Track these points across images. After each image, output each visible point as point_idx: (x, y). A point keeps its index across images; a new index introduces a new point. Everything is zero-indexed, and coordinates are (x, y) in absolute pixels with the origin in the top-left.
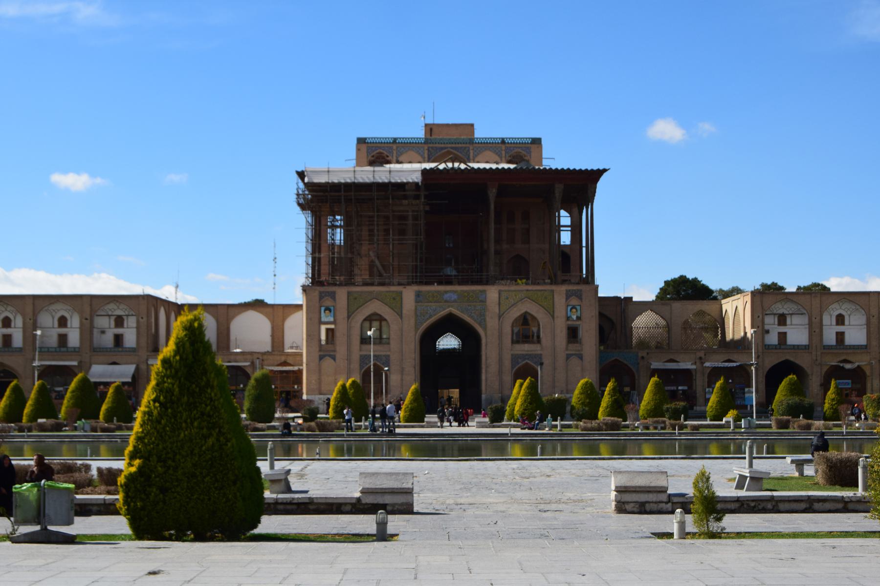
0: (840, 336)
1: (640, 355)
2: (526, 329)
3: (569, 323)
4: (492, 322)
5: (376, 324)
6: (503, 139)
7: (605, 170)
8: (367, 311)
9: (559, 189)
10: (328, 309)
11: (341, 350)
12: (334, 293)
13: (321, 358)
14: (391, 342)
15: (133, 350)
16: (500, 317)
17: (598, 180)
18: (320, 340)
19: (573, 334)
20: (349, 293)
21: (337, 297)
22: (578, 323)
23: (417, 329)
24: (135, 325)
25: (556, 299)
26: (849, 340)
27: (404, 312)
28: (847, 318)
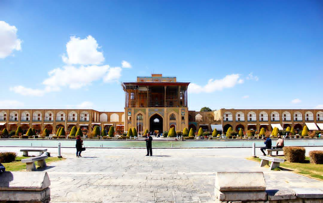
0: (239, 119)
2: (172, 118)
3: (182, 116)
4: (165, 116)
5: (140, 116)
7: (190, 83)
8: (138, 113)
9: (180, 87)
10: (130, 112)
13: (128, 123)
15: (88, 121)
16: (167, 114)
17: (188, 85)
18: (128, 119)
19: (183, 118)
22: (184, 116)
23: (149, 117)
26: (241, 120)
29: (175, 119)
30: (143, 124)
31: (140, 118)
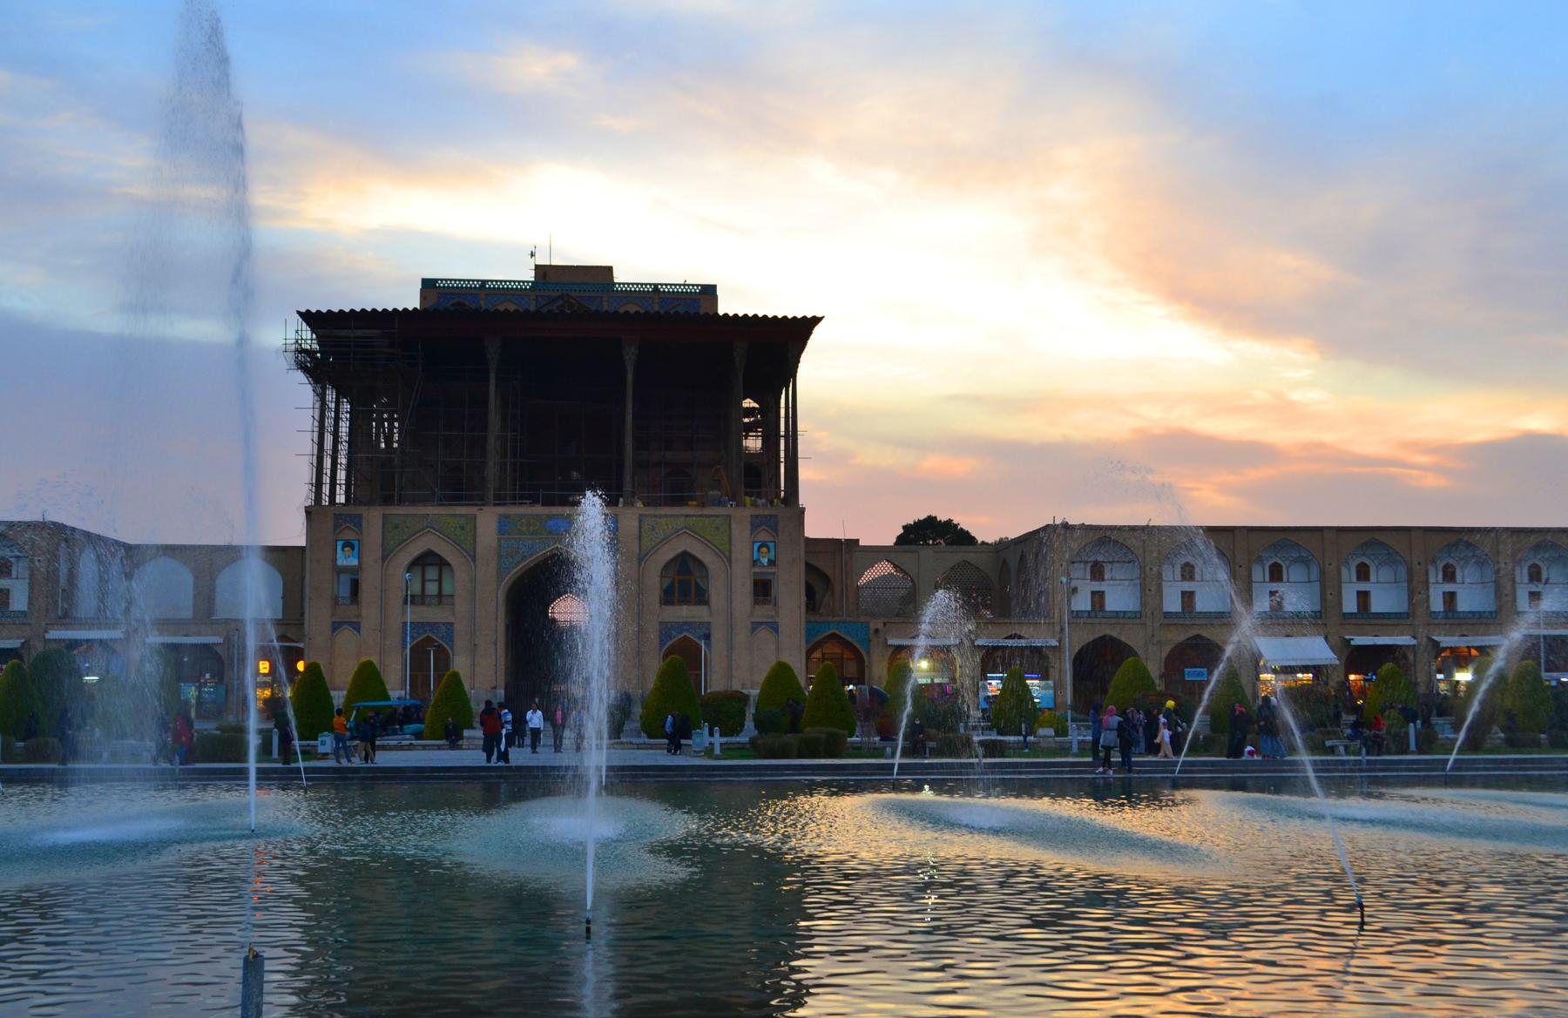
1: (872, 626)
5: (432, 573)
6: (656, 285)
8: (415, 549)
11: (369, 612)
12: (360, 516)
13: (336, 626)
14: (457, 601)
16: (640, 560)
19: (762, 590)
20: (385, 516)
21: (364, 524)
24: (27, 574)
25: (735, 532)
27: (479, 550)
28: (1197, 570)
29: (701, 598)
30: (450, 637)
31: (432, 588)
